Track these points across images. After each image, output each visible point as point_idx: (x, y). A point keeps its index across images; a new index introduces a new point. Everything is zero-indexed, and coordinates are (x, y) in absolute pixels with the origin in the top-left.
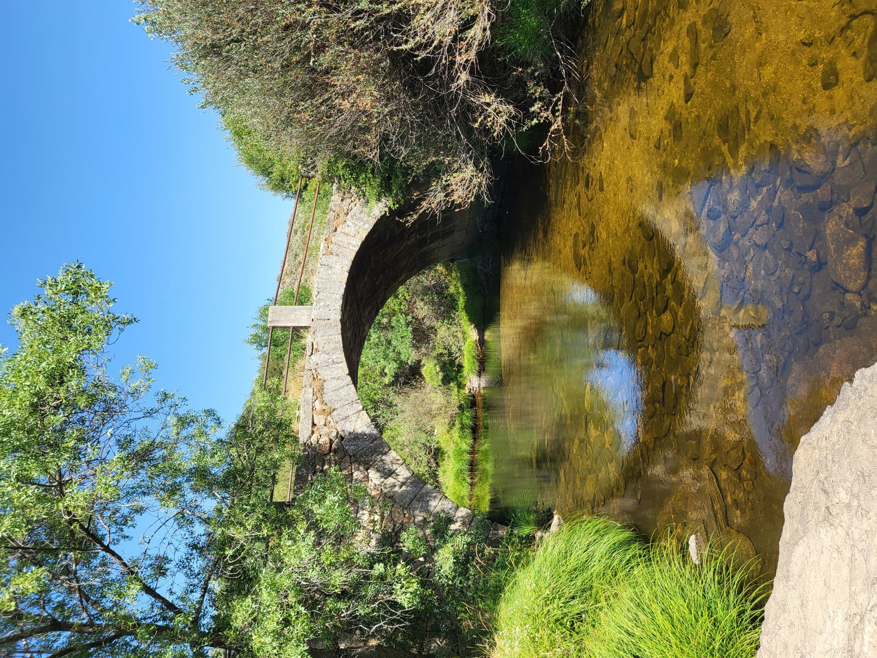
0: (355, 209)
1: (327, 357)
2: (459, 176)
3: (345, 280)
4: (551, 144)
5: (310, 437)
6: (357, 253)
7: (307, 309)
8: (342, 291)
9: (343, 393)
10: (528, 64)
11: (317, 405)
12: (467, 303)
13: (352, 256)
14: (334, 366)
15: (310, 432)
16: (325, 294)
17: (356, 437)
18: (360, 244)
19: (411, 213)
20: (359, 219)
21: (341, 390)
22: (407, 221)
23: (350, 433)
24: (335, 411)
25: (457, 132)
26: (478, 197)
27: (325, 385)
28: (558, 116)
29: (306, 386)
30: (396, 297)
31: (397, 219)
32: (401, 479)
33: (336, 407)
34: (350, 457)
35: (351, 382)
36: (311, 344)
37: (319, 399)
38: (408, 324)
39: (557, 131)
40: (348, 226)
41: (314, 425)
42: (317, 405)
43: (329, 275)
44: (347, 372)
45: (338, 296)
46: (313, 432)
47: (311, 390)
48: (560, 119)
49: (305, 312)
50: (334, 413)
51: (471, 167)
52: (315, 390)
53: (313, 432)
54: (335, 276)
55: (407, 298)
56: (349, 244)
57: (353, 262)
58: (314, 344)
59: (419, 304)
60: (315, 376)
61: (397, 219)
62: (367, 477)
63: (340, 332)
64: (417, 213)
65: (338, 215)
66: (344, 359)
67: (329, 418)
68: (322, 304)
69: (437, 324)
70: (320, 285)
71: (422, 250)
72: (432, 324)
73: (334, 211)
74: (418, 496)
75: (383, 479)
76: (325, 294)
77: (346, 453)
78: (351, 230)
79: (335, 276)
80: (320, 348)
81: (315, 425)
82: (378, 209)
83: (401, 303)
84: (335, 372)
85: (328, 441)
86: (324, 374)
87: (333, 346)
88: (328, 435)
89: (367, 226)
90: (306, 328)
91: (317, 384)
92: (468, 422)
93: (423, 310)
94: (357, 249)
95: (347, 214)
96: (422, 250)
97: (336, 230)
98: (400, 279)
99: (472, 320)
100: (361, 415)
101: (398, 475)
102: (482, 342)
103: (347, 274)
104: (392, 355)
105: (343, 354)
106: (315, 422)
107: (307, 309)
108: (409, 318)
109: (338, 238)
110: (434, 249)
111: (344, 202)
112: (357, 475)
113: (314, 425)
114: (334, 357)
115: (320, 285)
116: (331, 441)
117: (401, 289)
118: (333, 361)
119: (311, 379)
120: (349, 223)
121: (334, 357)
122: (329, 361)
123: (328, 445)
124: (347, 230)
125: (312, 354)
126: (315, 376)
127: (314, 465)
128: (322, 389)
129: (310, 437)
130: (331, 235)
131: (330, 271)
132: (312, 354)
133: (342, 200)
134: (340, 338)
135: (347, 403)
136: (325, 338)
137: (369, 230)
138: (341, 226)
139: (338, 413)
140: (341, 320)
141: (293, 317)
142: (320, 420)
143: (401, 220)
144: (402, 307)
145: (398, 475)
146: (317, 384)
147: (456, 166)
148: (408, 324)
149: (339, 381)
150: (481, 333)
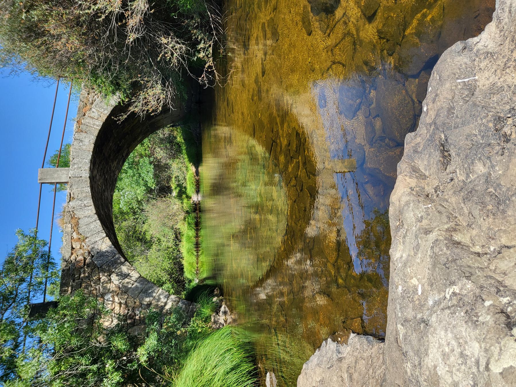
0: (97, 100)
1: (80, 202)
2: (151, 92)
3: (92, 150)
4: (207, 77)
5: (70, 257)
6: (100, 131)
7: (66, 170)
8: (90, 157)
9: (92, 226)
10: (192, 18)
11: (75, 235)
12: (186, 149)
13: (96, 133)
14: (86, 208)
15: (70, 254)
16: (78, 160)
17: (101, 254)
18: (101, 124)
19: (123, 114)
20: (101, 107)
21: (91, 224)
22: (119, 120)
23: (98, 253)
24: (87, 239)
25: (150, 61)
26: (165, 106)
27: (80, 221)
28: (210, 57)
29: (66, 223)
30: (142, 145)
31: (113, 118)
32: (134, 279)
33: (88, 236)
34: (98, 268)
35: (98, 219)
36: (69, 194)
37: (76, 231)
38: (151, 163)
39: (210, 67)
40: (93, 112)
41: (73, 248)
42: (75, 235)
43: (80, 146)
44: (95, 212)
45: (87, 161)
46: (72, 254)
47: (70, 226)
48: (211, 59)
49: (65, 172)
50: (87, 240)
51: (159, 86)
52: (73, 225)
53: (72, 254)
54: (84, 147)
55: (150, 146)
56: (94, 124)
57: (97, 137)
58: (72, 194)
59: (158, 150)
60: (73, 216)
61: (113, 118)
62: (110, 280)
63: (89, 185)
64: (126, 114)
65: (86, 104)
66: (92, 204)
67: (83, 244)
68: (76, 166)
69: (170, 162)
70: (75, 154)
71: (151, 122)
72: (167, 162)
73: (83, 102)
74: (144, 290)
75: (120, 281)
76: (78, 160)
77: (95, 266)
78: (95, 115)
79: (84, 147)
80: (76, 196)
81: (74, 248)
82: (114, 100)
83: (146, 150)
84: (87, 212)
85: (83, 258)
86: (79, 214)
87: (84, 195)
88: (83, 255)
89: (106, 112)
90: (67, 183)
91: (73, 221)
92: (192, 222)
93: (160, 154)
94: (99, 128)
95: (92, 103)
96: (151, 122)
97: (84, 115)
98: (138, 140)
99: (190, 161)
100: (105, 240)
101: (131, 277)
102: (197, 173)
103: (93, 145)
104: (142, 182)
105: (92, 200)
106: (74, 246)
107: (66, 170)
108: (152, 159)
109: (86, 120)
110: (160, 120)
111: (90, 96)
112: (103, 278)
113: (73, 248)
114: (85, 202)
115: (75, 154)
116: (85, 259)
117: (146, 141)
118: (85, 205)
119: (70, 218)
120: (93, 110)
121: (85, 202)
122: (82, 205)
123: (83, 261)
124: (92, 115)
125: (70, 201)
126: (73, 216)
127: (74, 275)
128: (77, 224)
129: (70, 257)
130: (81, 118)
131: (81, 144)
132: (70, 201)
133: (88, 94)
134: (89, 189)
135: (95, 232)
136: (79, 189)
137: (108, 115)
138: (88, 112)
139: (89, 240)
140: (90, 177)
141: (56, 176)
142: (77, 245)
143: (115, 119)
144: (147, 152)
145: (131, 277)
146: (73, 221)
147: (150, 84)
148: (151, 163)
149: (89, 219)
150: (197, 167)
